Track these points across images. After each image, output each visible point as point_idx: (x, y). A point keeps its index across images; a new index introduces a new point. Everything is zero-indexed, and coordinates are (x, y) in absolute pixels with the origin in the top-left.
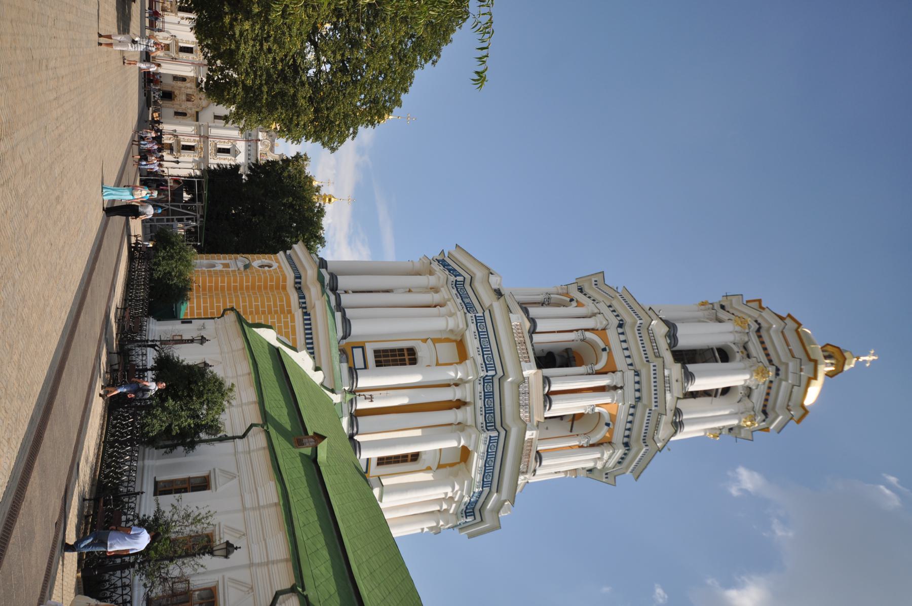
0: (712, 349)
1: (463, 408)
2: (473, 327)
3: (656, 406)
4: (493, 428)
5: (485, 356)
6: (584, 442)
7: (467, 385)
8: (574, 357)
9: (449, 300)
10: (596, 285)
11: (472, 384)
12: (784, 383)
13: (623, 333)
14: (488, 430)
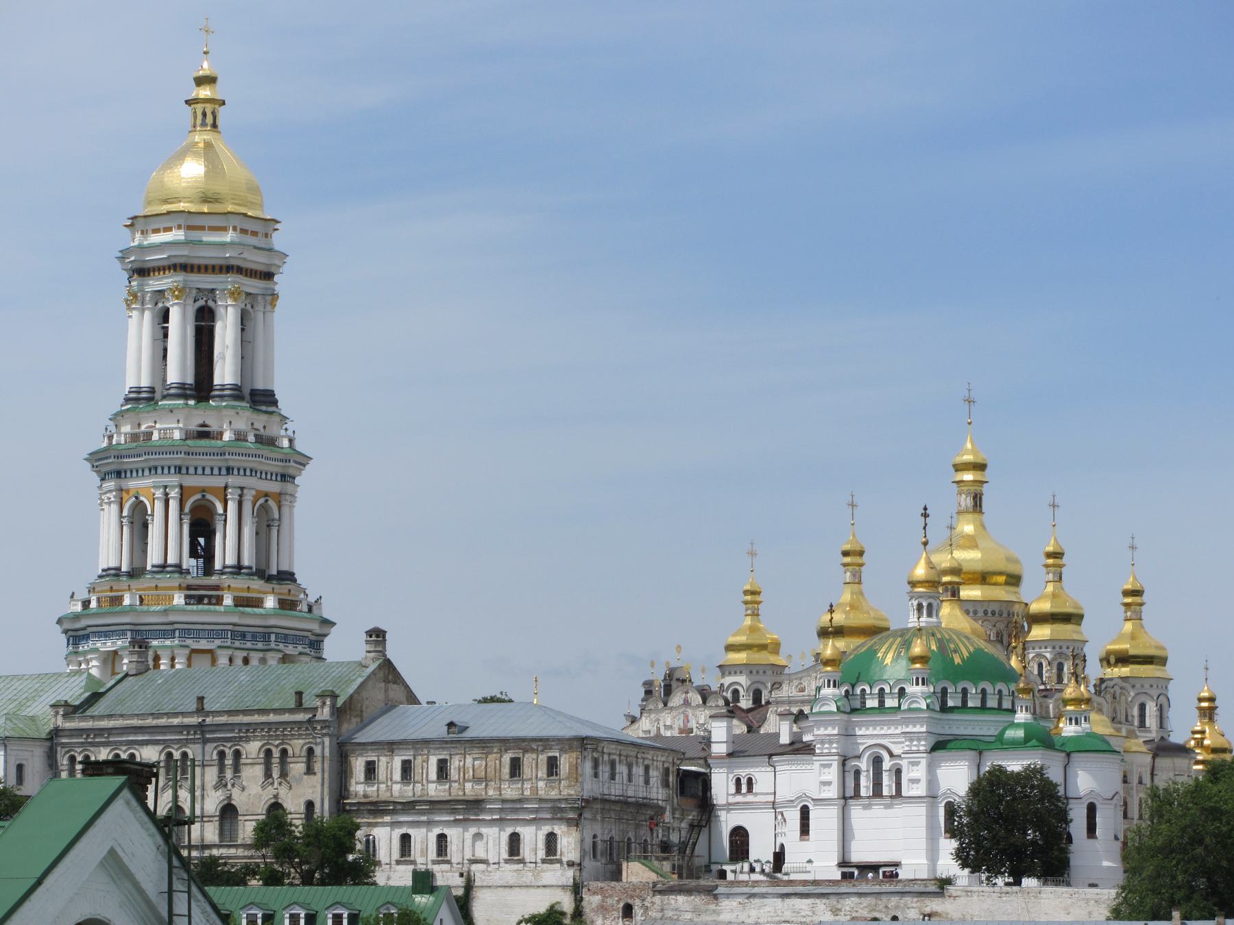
13: (126, 472)
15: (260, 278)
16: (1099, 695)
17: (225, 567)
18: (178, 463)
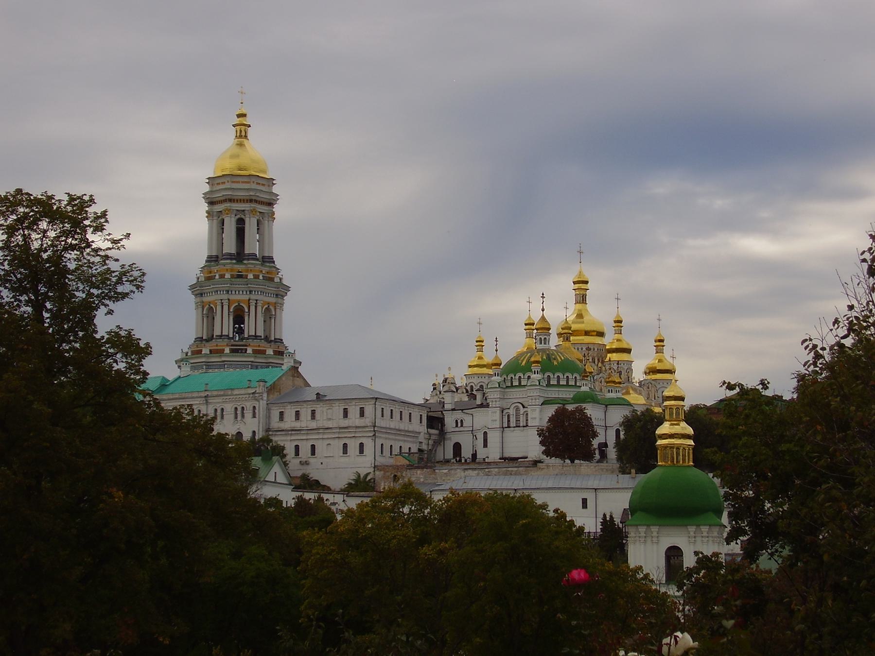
15: (266, 205)
16: (641, 387)
17: (249, 336)
18: (227, 289)
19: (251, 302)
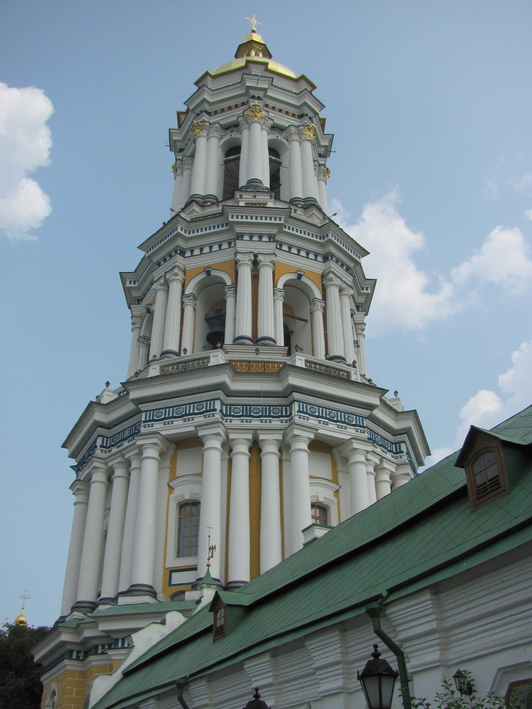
0: (226, 162)
1: (261, 444)
2: (158, 426)
3: (280, 220)
4: (288, 408)
5: (196, 411)
6: (319, 305)
7: (231, 436)
8: (217, 310)
9: (123, 455)
10: (134, 283)
11: (229, 431)
12: (269, 93)
14: (291, 414)
19: (331, 280)
